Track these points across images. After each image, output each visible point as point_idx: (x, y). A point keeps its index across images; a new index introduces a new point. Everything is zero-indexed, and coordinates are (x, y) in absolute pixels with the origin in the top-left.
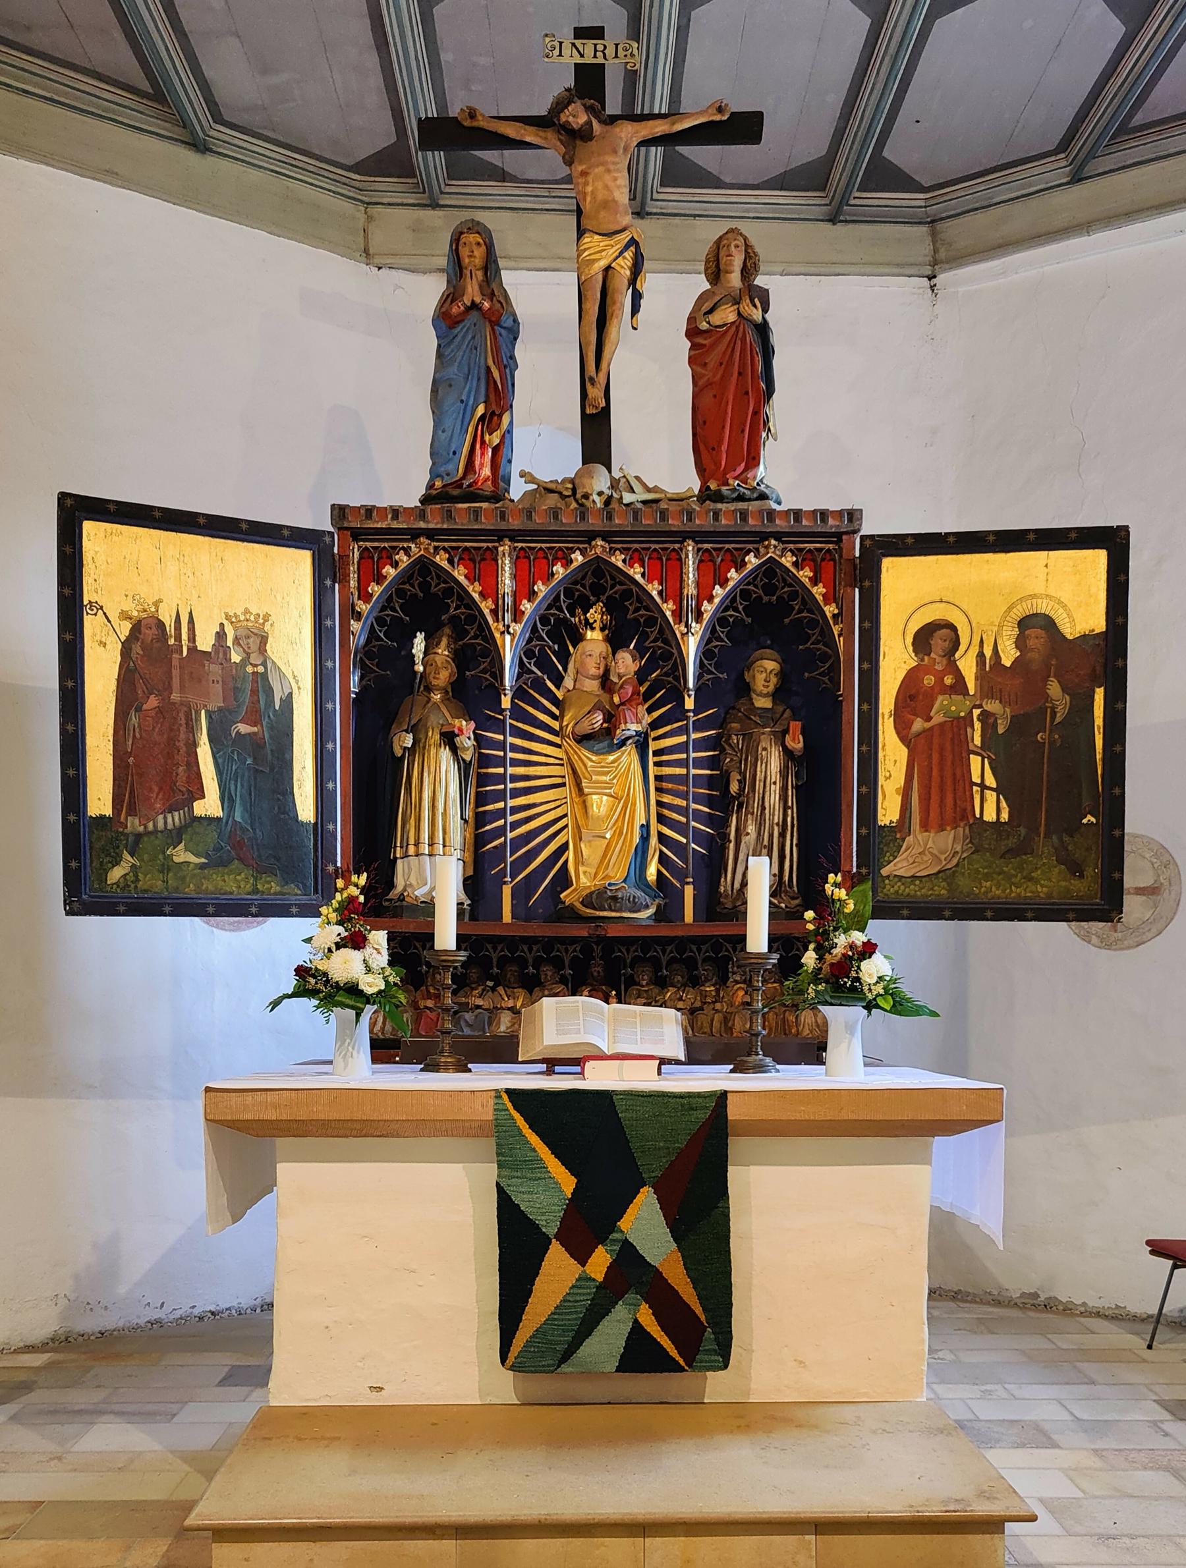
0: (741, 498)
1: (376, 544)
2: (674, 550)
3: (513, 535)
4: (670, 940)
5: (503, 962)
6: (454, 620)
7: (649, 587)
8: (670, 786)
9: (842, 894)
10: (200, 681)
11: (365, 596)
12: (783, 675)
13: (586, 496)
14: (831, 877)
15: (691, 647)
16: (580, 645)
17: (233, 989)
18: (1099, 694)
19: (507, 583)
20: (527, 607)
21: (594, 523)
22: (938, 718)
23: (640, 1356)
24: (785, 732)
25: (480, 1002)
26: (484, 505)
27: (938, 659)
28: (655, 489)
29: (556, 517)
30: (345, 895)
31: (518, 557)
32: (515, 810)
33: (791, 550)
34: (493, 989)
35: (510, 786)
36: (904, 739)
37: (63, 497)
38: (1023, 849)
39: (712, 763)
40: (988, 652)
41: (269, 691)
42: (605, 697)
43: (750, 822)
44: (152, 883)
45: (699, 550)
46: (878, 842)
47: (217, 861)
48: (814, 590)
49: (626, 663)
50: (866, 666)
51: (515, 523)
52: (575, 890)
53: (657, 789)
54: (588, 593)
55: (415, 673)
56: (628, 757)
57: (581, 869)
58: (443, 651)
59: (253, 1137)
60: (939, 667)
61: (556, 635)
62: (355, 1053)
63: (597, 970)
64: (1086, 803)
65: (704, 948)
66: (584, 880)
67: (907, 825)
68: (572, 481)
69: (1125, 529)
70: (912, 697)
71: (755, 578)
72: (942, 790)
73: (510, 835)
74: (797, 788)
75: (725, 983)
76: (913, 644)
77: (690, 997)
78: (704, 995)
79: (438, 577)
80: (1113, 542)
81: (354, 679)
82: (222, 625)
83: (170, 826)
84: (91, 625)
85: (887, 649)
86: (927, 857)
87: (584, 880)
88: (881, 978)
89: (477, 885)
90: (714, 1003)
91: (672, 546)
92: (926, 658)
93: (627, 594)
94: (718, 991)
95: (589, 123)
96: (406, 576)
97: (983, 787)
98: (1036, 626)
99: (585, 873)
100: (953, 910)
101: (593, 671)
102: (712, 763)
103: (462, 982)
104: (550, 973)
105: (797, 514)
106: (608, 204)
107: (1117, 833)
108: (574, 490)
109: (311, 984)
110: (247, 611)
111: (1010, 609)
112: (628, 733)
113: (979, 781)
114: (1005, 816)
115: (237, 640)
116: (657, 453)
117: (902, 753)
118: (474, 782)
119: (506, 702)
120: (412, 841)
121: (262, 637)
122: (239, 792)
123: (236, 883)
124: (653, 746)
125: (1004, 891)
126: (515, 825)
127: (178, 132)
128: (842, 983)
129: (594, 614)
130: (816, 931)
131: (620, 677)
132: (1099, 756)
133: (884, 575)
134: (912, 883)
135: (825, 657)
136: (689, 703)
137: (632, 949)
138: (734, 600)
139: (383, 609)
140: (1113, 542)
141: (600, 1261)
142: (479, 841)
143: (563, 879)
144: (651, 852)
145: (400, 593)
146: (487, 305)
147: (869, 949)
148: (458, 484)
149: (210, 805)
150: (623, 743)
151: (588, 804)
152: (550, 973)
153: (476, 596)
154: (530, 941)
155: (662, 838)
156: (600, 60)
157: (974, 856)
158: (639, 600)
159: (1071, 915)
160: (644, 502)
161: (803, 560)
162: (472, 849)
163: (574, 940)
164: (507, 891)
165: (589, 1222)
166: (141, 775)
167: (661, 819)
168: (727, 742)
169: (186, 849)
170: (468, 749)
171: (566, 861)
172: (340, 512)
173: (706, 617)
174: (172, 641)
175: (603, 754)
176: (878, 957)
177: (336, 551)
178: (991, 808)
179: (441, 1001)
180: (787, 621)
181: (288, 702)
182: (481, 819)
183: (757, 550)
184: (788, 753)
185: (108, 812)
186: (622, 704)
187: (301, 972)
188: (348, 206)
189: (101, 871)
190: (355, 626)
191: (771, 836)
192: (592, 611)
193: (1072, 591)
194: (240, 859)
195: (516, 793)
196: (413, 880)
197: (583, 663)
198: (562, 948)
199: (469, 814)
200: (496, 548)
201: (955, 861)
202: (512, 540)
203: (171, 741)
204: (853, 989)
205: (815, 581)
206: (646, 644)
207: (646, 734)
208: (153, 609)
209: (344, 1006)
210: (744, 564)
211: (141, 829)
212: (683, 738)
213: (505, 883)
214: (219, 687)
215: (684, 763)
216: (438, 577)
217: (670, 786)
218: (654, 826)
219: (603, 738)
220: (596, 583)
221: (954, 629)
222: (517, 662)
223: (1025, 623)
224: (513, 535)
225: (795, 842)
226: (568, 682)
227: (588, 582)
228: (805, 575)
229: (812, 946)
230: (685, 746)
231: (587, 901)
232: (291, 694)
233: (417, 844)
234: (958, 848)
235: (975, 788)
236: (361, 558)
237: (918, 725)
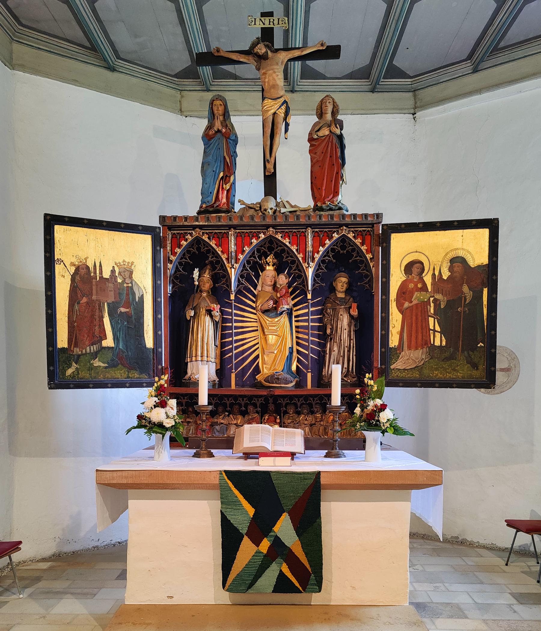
0: (331, 209)
1: (178, 232)
2: (303, 232)
3: (235, 227)
4: (301, 396)
5: (232, 405)
6: (211, 262)
7: (292, 248)
8: (302, 330)
9: (371, 382)
10: (104, 290)
11: (174, 254)
12: (350, 284)
13: (265, 210)
14: (367, 374)
15: (310, 273)
16: (264, 272)
18: (485, 291)
19: (233, 247)
20: (241, 257)
21: (269, 221)
22: (415, 302)
23: (282, 585)
24: (350, 308)
25: (222, 421)
26: (223, 215)
27: (415, 277)
28: (295, 206)
29: (253, 219)
30: (159, 384)
31: (237, 236)
32: (237, 341)
33: (352, 231)
34: (228, 416)
35: (234, 331)
36: (400, 311)
37: (46, 215)
38: (452, 357)
39: (320, 320)
40: (437, 273)
41: (134, 294)
42: (274, 294)
43: (335, 346)
44: (85, 375)
45: (313, 231)
46: (389, 354)
47: (112, 365)
48: (362, 248)
49: (283, 280)
50: (384, 280)
51: (235, 222)
52: (262, 375)
53: (296, 332)
54: (267, 251)
55: (195, 285)
56: (284, 319)
57: (264, 366)
58: (207, 276)
59: (117, 489)
60: (415, 280)
61: (254, 268)
62: (163, 452)
63: (271, 407)
64: (479, 337)
65: (316, 399)
66: (265, 371)
67: (401, 348)
68: (260, 204)
69: (497, 220)
70: (404, 293)
71: (337, 243)
72: (417, 332)
73: (234, 352)
74: (355, 331)
75: (325, 413)
76: (404, 270)
77: (310, 418)
78: (316, 418)
79: (204, 245)
80: (492, 225)
81: (169, 289)
82: (113, 267)
83: (92, 351)
84: (58, 268)
85: (393, 273)
86: (410, 361)
87: (265, 371)
88: (388, 420)
89: (222, 372)
90: (321, 421)
91: (302, 230)
92: (410, 276)
93: (283, 251)
94: (322, 416)
95: (267, 52)
96: (191, 245)
97: (434, 331)
98: (458, 262)
99: (266, 367)
100: (421, 383)
101: (269, 283)
102: (320, 320)
103: (213, 414)
104: (252, 409)
105: (355, 216)
106: (274, 86)
107: (493, 351)
108: (260, 207)
109: (144, 423)
110: (124, 261)
111: (446, 255)
112: (283, 309)
113: (433, 328)
114: (444, 343)
115: (120, 273)
116: (296, 191)
117: (400, 316)
118: (220, 330)
119: (232, 297)
120: (194, 355)
121: (131, 271)
122: (121, 336)
123: (120, 374)
124: (294, 314)
125: (443, 375)
126: (237, 347)
127: (102, 63)
128: (372, 421)
129: (270, 259)
130: (361, 399)
131: (281, 285)
132: (485, 318)
133: (392, 241)
134: (404, 372)
135: (367, 276)
136: (309, 296)
137: (285, 400)
138: (328, 252)
139: (181, 259)
140: (492, 225)
141: (265, 545)
142: (223, 354)
143: (257, 370)
144: (294, 358)
145: (189, 252)
146: (224, 130)
147: (383, 407)
148: (212, 206)
149: (109, 342)
150: (281, 313)
151: (267, 339)
152: (252, 409)
153: (219, 253)
154: (243, 397)
155: (298, 352)
156: (272, 26)
157: (430, 361)
158: (288, 253)
159: (473, 386)
160: (290, 212)
161: (358, 235)
162: (219, 358)
163: (261, 396)
164: (233, 376)
165: (261, 528)
166: (80, 330)
167: (298, 344)
168: (326, 312)
169: (99, 361)
170: (217, 316)
171: (258, 362)
172: (163, 219)
173: (316, 260)
174: (92, 274)
175: (273, 318)
176: (387, 411)
177: (161, 235)
178: (438, 340)
180: (350, 261)
181: (142, 298)
182: (223, 345)
183: (338, 231)
184: (351, 316)
185: (66, 346)
186: (281, 297)
187: (140, 417)
188: (173, 92)
189: (63, 370)
190: (170, 266)
191: (344, 352)
192: (268, 258)
193: (474, 247)
194: (122, 364)
195: (237, 334)
196: (194, 371)
197: (265, 279)
198: (256, 399)
199: (218, 343)
200: (228, 233)
201: (422, 362)
202: (235, 229)
203: (92, 316)
204: (376, 425)
205: (362, 244)
206: (291, 272)
207: (292, 309)
208: (84, 261)
209: (156, 433)
210: (332, 237)
211: (80, 353)
212: (307, 311)
213: (232, 372)
214: (113, 293)
215: (307, 321)
216: (204, 245)
217: (302, 330)
218: (295, 347)
219: (273, 311)
220: (271, 246)
221: (422, 263)
222: (237, 280)
223: (453, 261)
224: (235, 227)
225: (354, 354)
226: (259, 288)
227: (266, 246)
228: (358, 241)
229: (359, 405)
230: (308, 313)
231: (266, 380)
232: (143, 295)
233: (196, 356)
234: (424, 357)
235: (431, 331)
236: (172, 238)
237: (407, 305)
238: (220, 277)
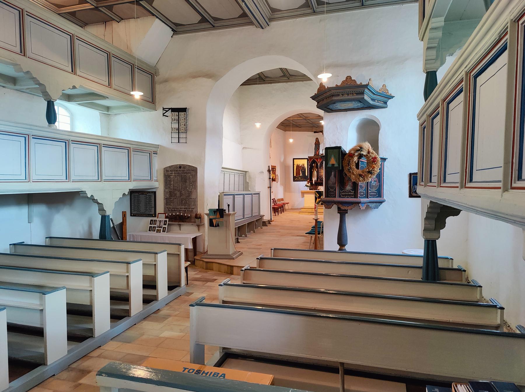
17: (303, 185)
59: (303, 193)
89: (317, 179)
109: (306, 186)
123: (302, 179)
165: (319, 197)
179: (313, 186)
189: (295, 179)
238: (317, 165)
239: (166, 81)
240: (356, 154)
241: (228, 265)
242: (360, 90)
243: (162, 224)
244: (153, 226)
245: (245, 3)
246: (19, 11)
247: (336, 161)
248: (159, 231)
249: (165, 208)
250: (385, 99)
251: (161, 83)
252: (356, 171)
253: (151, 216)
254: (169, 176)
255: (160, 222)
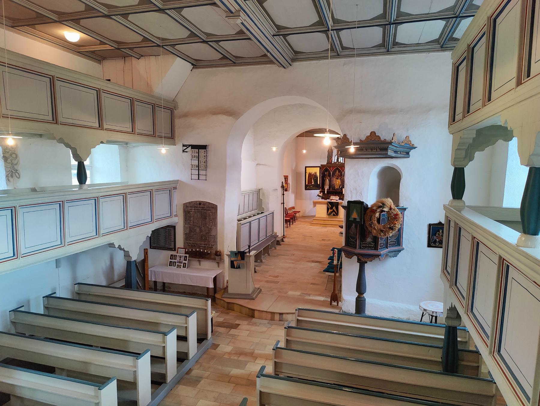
23: (334, 215)
59: (315, 204)
109: (318, 195)
165: (331, 208)
189: (307, 188)
219: (337, 179)
220: (337, 169)
238: (330, 173)
239: (185, 115)
240: (378, 210)
241: (249, 309)
242: (386, 145)
243: (182, 259)
244: (173, 261)
245: (270, 53)
246: (50, 78)
247: (358, 216)
248: (179, 266)
249: (184, 243)
250: (408, 150)
251: (180, 117)
252: (377, 226)
253: (171, 249)
254: (189, 212)
255: (180, 257)
